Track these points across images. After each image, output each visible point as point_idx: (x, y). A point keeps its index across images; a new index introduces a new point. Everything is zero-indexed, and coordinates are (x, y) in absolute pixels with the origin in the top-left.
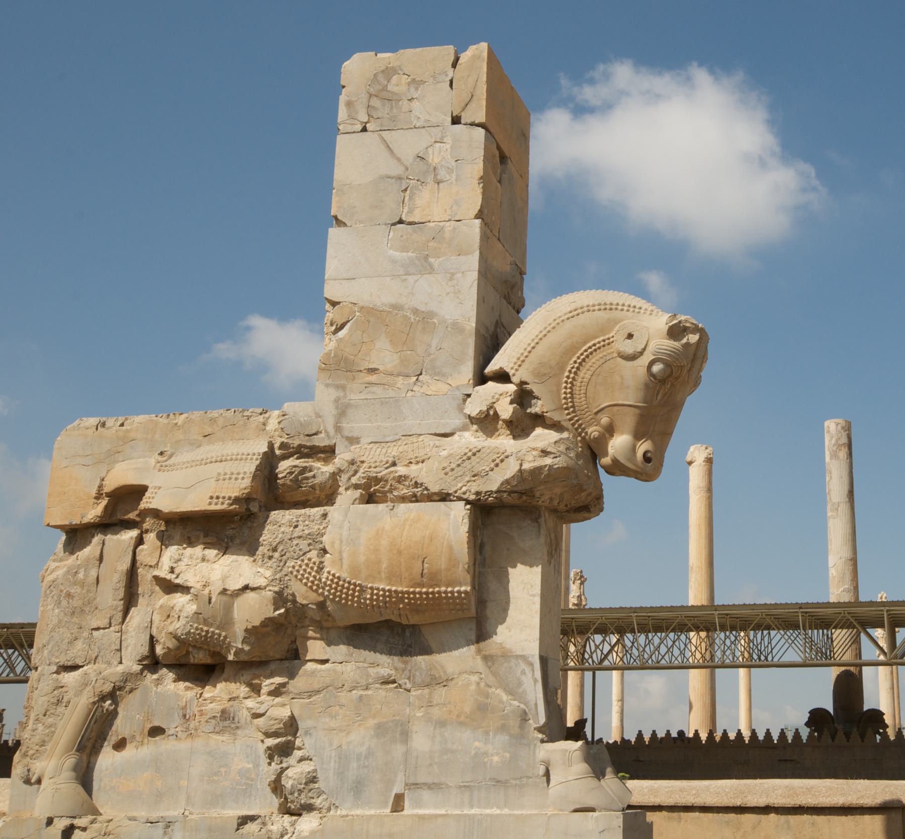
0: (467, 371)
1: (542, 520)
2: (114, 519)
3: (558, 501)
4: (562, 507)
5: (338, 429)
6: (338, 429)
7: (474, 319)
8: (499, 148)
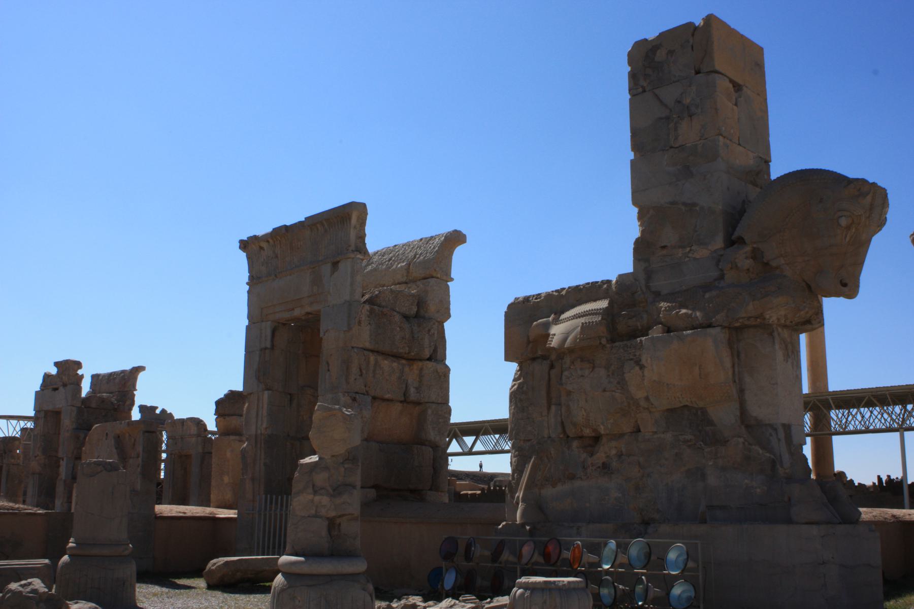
1: (776, 334)
3: (784, 320)
4: (788, 323)
5: (648, 287)
6: (648, 287)
8: (731, 81)
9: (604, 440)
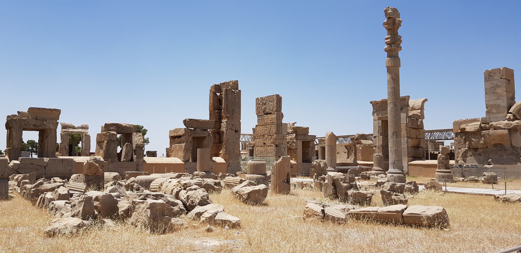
0: (506, 112)
2: (462, 132)
5: (489, 120)
7: (506, 105)
8: (508, 80)
9: (479, 149)
